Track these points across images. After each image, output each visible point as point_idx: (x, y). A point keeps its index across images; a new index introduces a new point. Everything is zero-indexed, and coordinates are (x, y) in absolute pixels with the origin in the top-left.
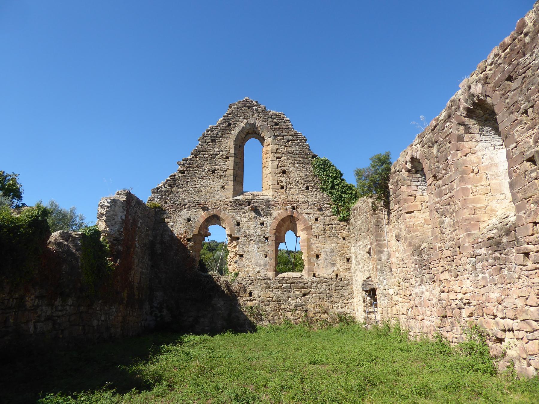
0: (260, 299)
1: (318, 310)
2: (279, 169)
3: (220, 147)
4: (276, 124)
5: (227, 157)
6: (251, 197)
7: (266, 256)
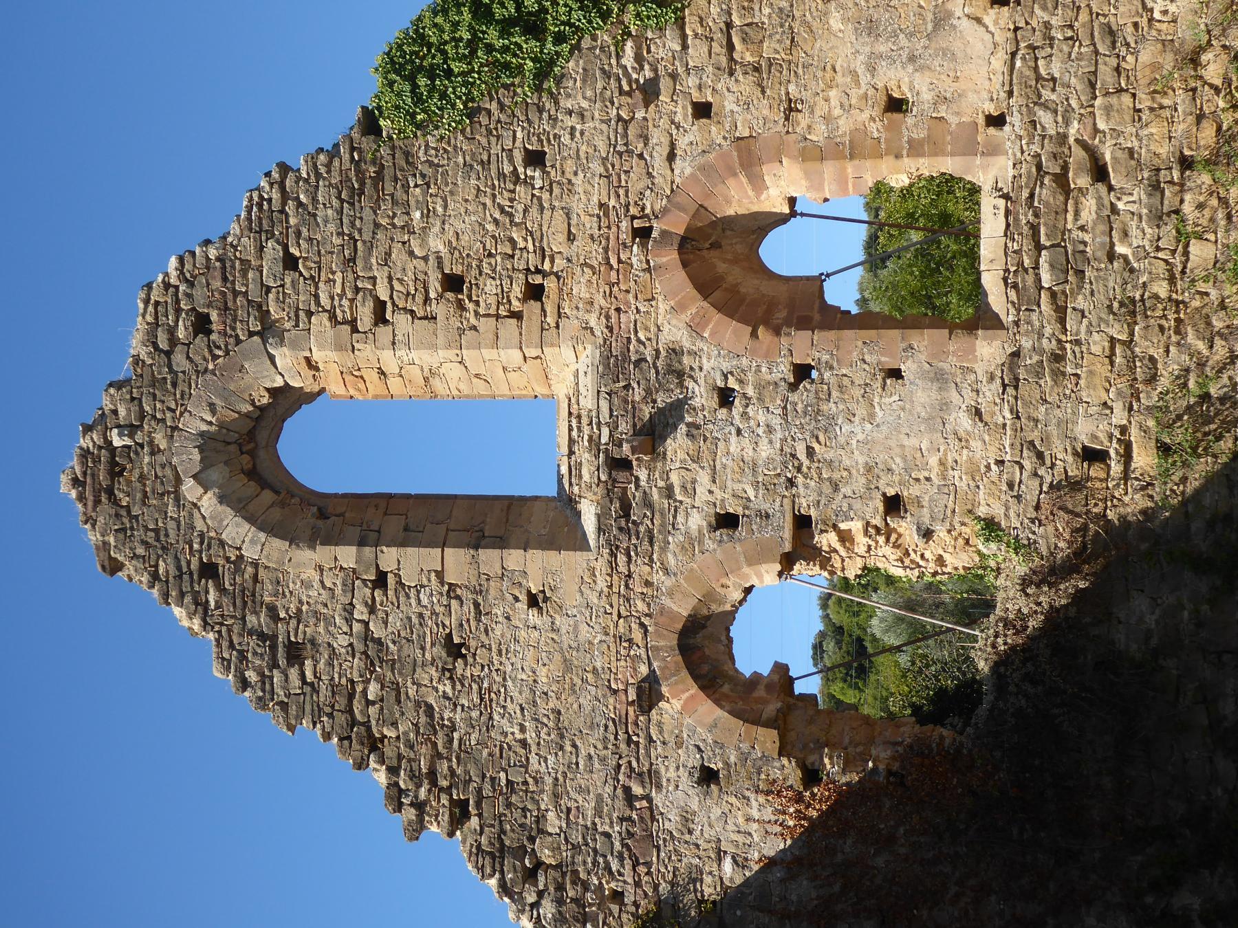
0: (1118, 407)
1: (1181, 98)
2: (439, 309)
3: (330, 621)
4: (201, 325)
5: (381, 581)
6: (584, 455)
7: (896, 374)
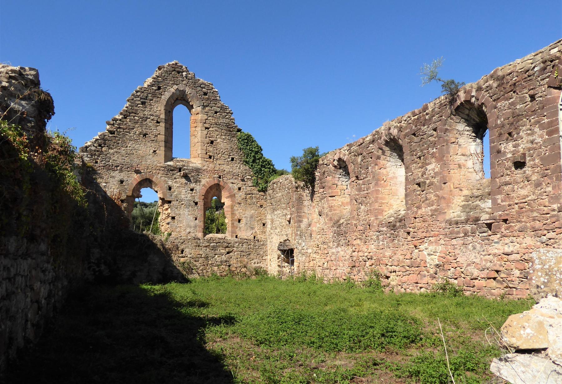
0: (191, 256)
3: (150, 111)
4: (205, 94)
5: (158, 122)
6: (181, 163)
7: (196, 219)
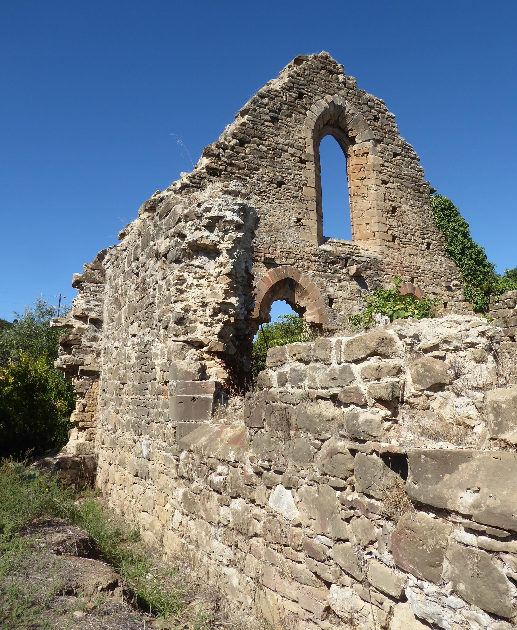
5: (302, 161)
